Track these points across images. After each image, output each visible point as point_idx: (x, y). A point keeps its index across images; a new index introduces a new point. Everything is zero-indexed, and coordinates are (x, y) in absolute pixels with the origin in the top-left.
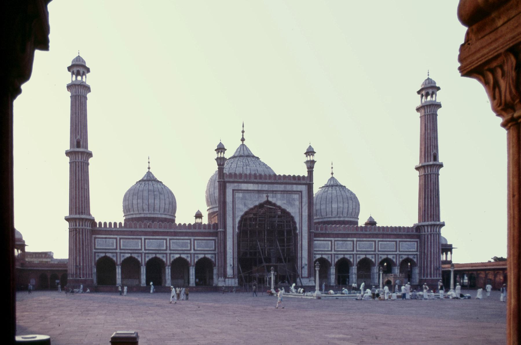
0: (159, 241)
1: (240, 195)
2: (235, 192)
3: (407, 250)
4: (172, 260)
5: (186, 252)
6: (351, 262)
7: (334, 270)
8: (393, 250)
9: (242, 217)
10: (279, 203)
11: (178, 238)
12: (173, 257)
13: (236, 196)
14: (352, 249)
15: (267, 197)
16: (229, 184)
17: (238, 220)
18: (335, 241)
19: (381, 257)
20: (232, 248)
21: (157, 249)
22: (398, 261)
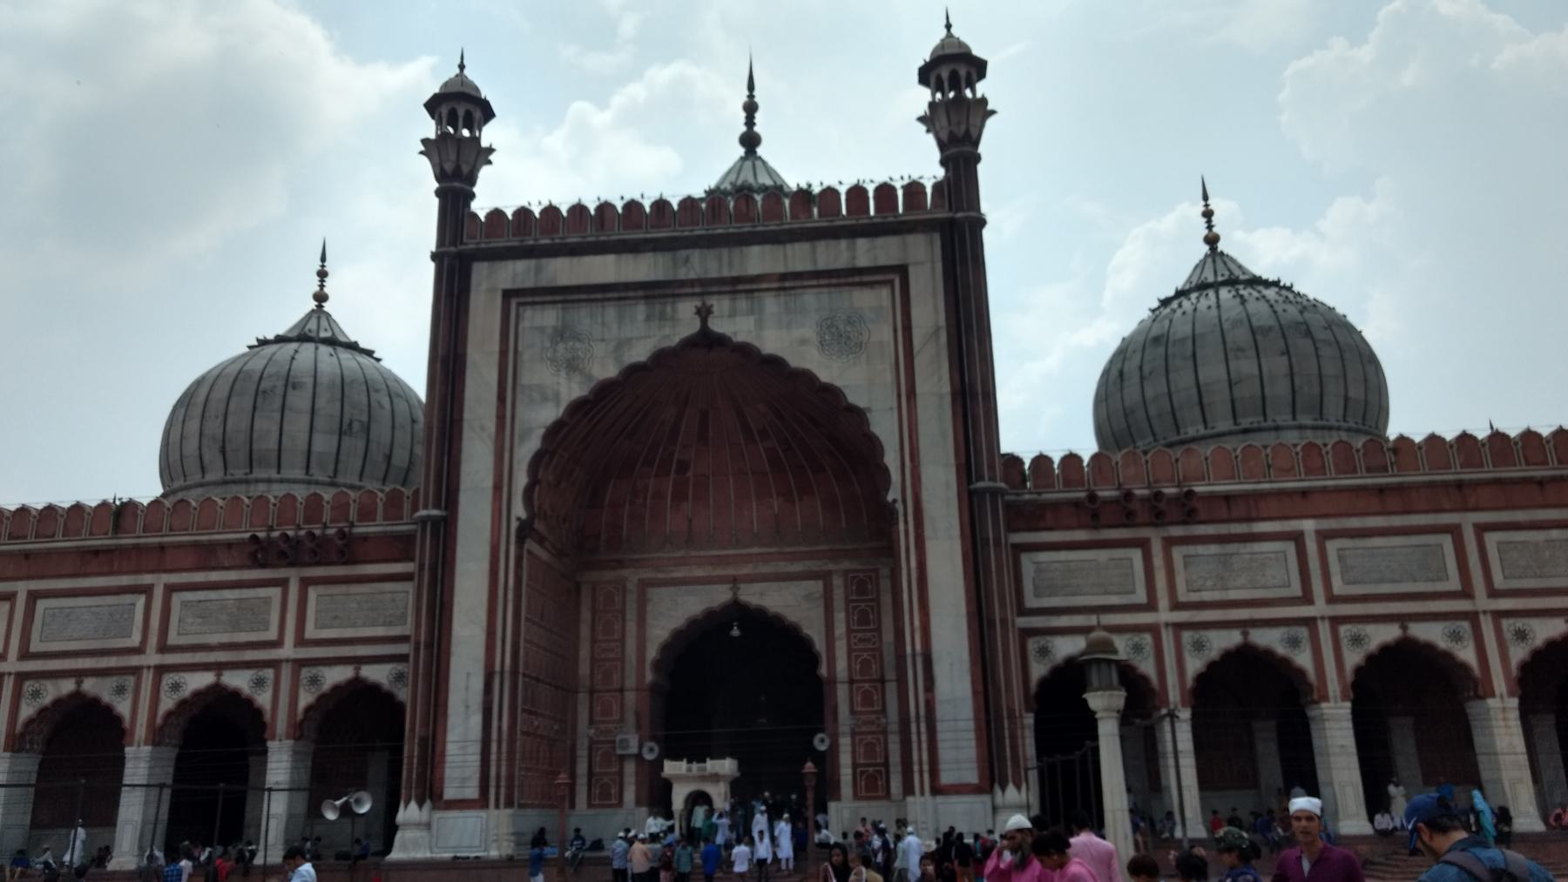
1: (548, 317)
2: (519, 304)
4: (167, 703)
5: (250, 655)
6: (1301, 673)
9: (555, 432)
10: (772, 342)
11: (215, 576)
12: (176, 687)
13: (525, 324)
14: (1296, 590)
15: (704, 313)
16: (485, 264)
17: (527, 449)
18: (1169, 542)
19: (1521, 635)
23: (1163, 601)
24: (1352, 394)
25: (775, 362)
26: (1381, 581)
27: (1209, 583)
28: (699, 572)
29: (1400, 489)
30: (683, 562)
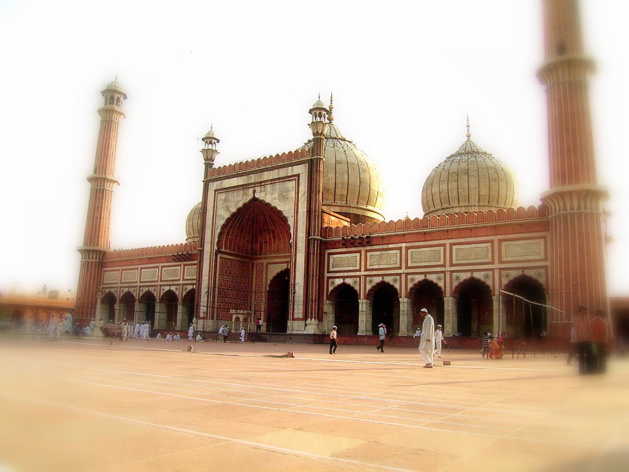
0: (153, 269)
3: (520, 258)
5: (175, 283)
6: (396, 290)
7: (364, 306)
8: (486, 261)
9: (224, 227)
10: (268, 199)
11: (169, 264)
15: (254, 192)
17: (218, 231)
18: (367, 251)
19: (458, 278)
20: (208, 274)
21: (151, 280)
22: (497, 284)
23: (363, 269)
24: (482, 193)
25: (268, 205)
26: (422, 262)
27: (376, 263)
28: (280, 260)
29: (430, 233)
30: (276, 257)
